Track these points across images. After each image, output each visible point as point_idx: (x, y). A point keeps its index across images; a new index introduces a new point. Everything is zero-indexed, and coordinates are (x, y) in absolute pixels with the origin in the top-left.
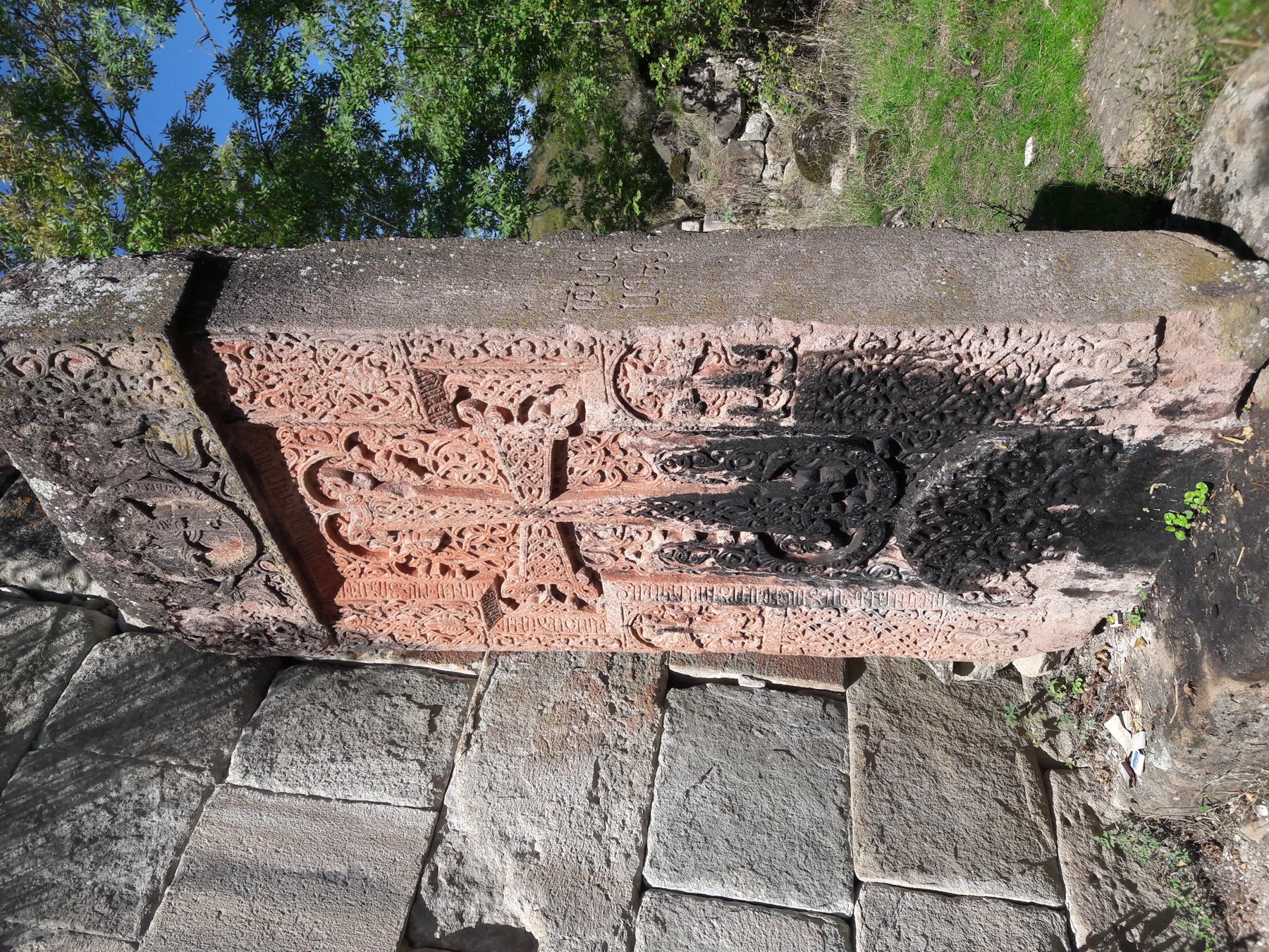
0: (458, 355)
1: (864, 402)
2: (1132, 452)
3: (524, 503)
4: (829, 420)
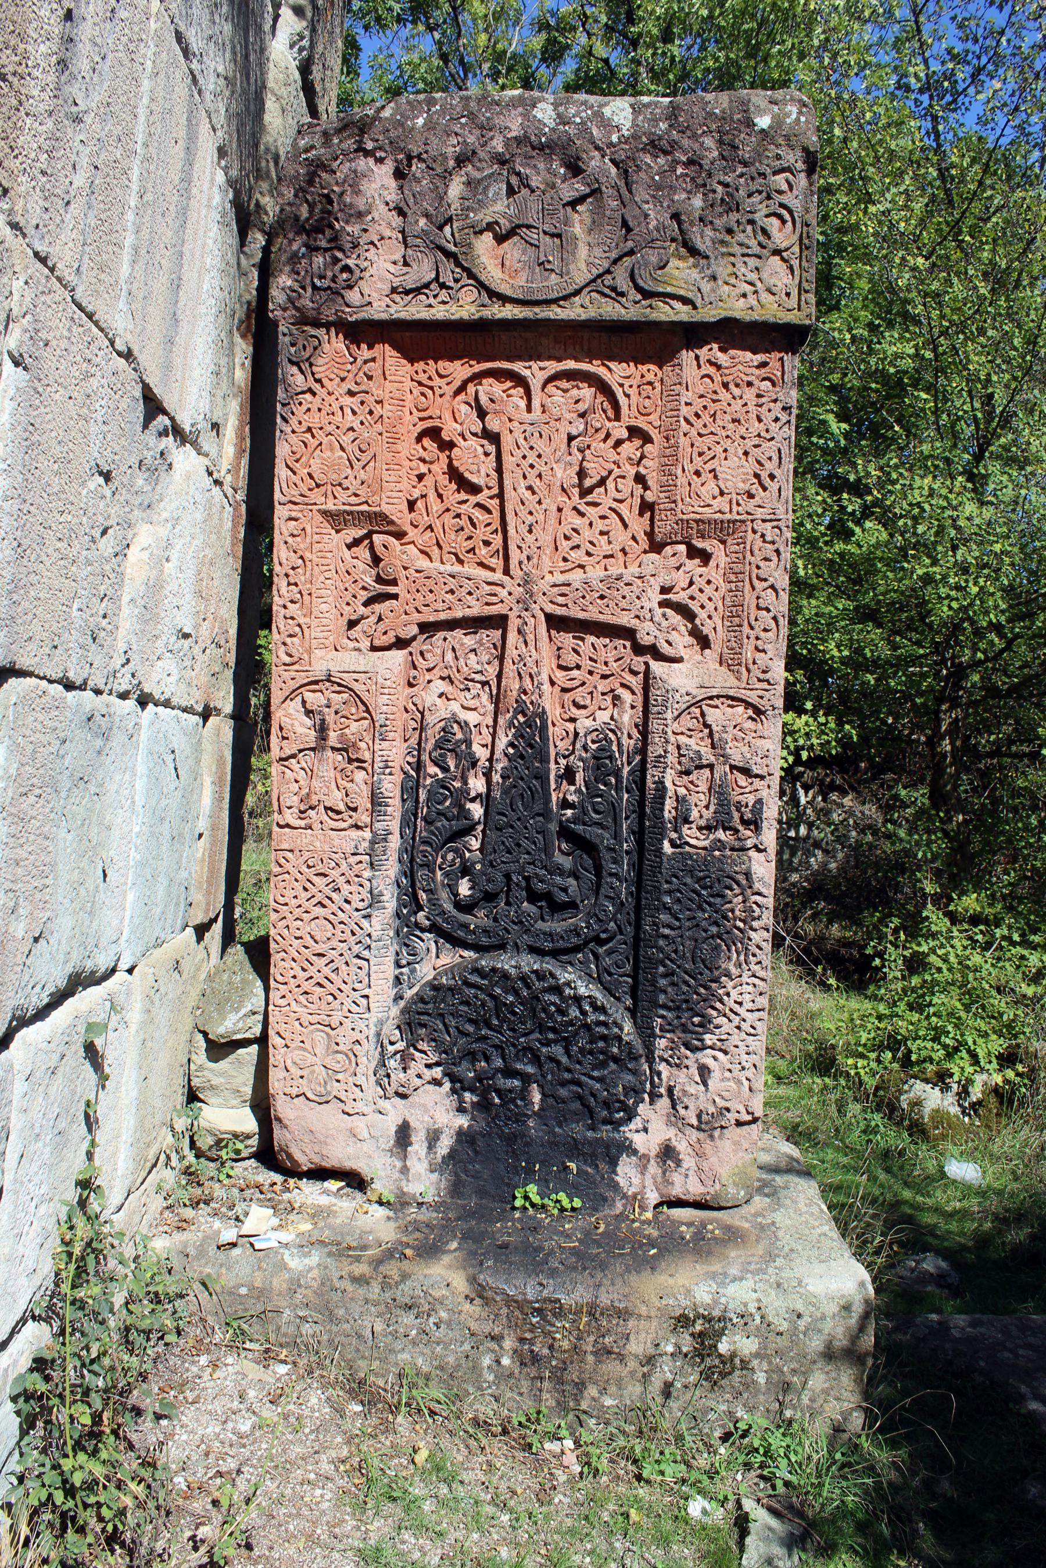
0: (762, 564)
1: (689, 910)
2: (617, 1136)
3: (544, 585)
4: (667, 882)
